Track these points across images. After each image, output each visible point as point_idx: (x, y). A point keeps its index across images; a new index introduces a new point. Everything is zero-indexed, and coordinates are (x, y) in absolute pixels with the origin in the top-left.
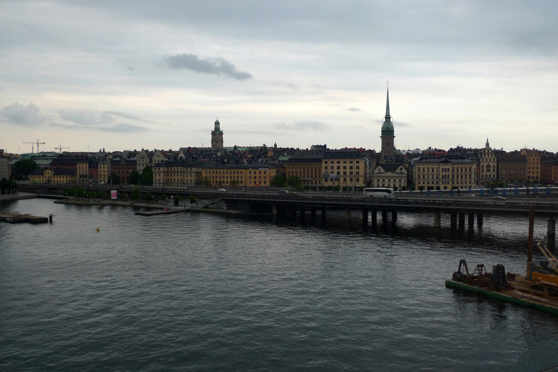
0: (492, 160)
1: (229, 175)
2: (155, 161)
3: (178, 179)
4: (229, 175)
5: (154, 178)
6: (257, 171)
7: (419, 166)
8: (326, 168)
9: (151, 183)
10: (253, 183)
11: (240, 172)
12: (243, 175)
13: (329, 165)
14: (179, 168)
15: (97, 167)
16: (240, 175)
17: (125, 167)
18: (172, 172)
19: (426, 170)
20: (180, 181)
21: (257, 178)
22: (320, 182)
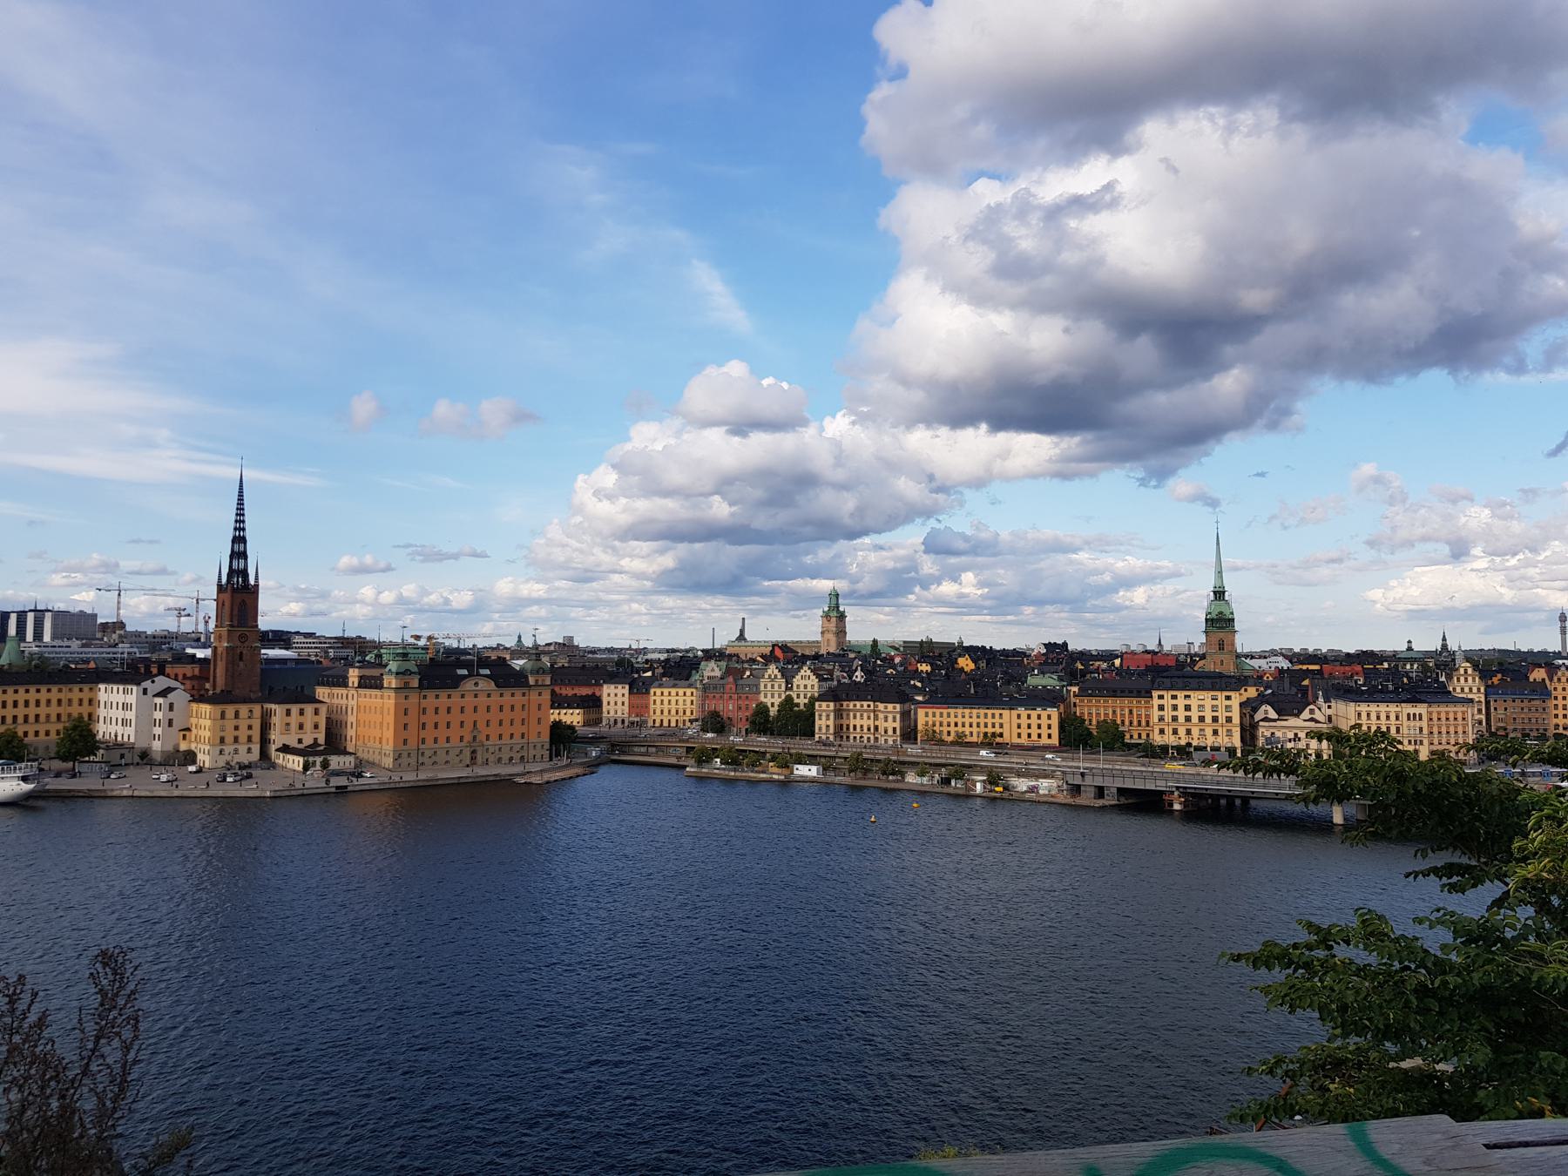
4: (975, 720)
5: (818, 723)
6: (1034, 714)
9: (810, 734)
10: (1024, 736)
13: (1168, 701)
19: (1373, 716)
21: (1034, 727)
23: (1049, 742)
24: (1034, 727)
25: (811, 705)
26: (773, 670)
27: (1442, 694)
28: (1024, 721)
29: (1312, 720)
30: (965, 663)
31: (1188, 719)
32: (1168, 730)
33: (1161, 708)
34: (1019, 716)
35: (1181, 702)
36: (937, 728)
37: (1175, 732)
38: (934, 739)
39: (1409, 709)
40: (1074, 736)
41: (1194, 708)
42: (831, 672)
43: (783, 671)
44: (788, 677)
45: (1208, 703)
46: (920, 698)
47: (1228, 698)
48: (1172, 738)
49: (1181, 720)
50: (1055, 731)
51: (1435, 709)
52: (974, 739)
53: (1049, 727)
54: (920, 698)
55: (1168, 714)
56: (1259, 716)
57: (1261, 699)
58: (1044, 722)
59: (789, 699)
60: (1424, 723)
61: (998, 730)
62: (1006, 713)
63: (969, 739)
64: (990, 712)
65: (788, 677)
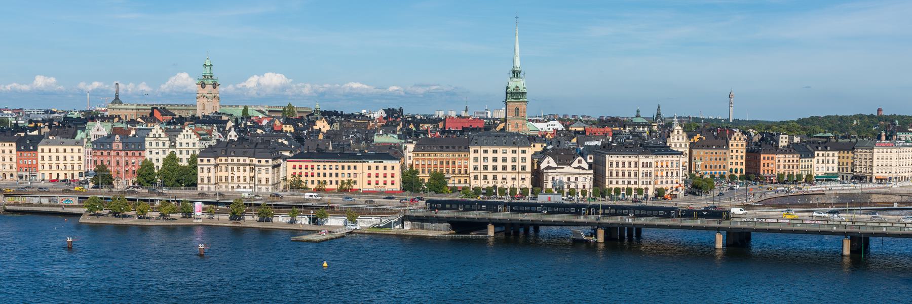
0: (683, 145)
1: (334, 172)
2: (181, 144)
3: (239, 177)
4: (334, 172)
5: (200, 175)
6: (381, 166)
10: (373, 183)
12: (358, 171)
13: (481, 155)
14: (242, 159)
15: (35, 150)
16: (352, 171)
17: (122, 154)
18: (228, 165)
20: (242, 181)
21: (381, 176)
24: (381, 176)
25: (193, 160)
26: (157, 129)
27: (665, 150)
28: (373, 172)
29: (579, 167)
30: (322, 125)
31: (495, 168)
32: (481, 176)
33: (476, 159)
34: (369, 168)
36: (303, 178)
37: (485, 178)
39: (643, 159)
42: (210, 133)
43: (167, 131)
45: (509, 156)
46: (287, 154)
47: (524, 152)
48: (483, 182)
49: (490, 168)
50: (397, 179)
51: (660, 158)
52: (334, 186)
54: (287, 154)
55: (481, 164)
56: (543, 165)
57: (544, 153)
58: (389, 172)
59: (172, 155)
60: (652, 169)
61: (352, 178)
62: (359, 165)
63: (328, 186)
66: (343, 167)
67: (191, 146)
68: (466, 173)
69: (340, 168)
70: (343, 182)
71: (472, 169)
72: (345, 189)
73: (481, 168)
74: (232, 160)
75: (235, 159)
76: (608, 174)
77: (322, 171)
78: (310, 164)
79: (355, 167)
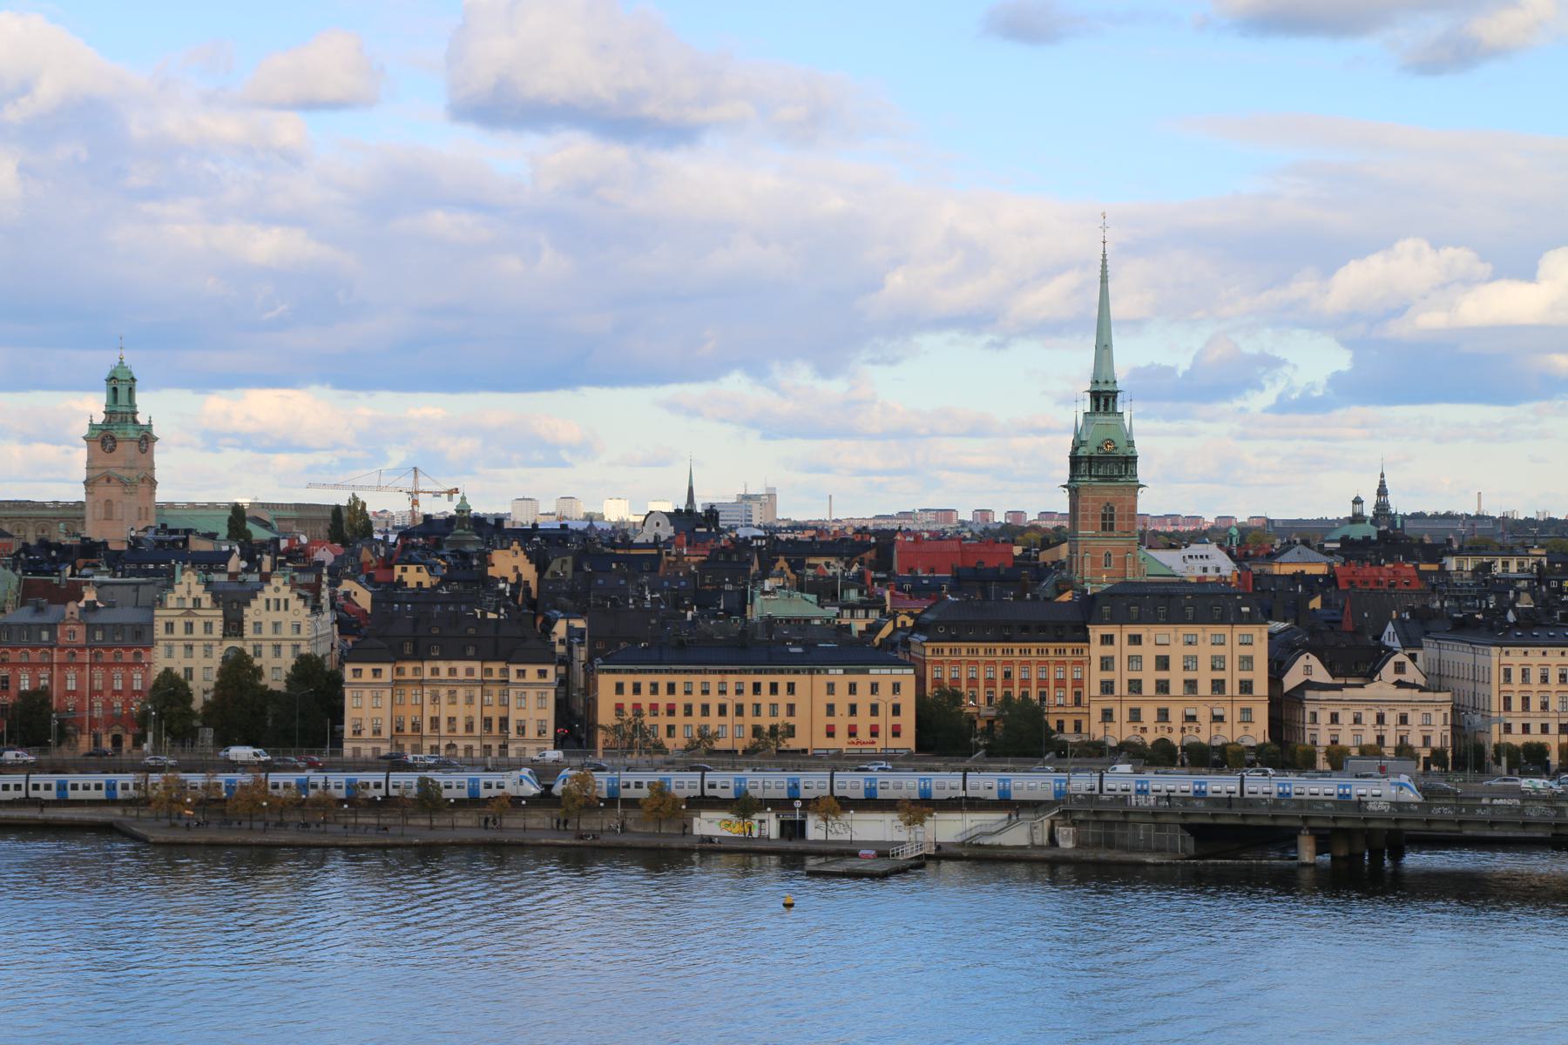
1: (731, 700)
2: (258, 626)
3: (451, 720)
6: (863, 682)
7: (1505, 660)
8: (1106, 663)
9: (338, 741)
11: (782, 688)
13: (1121, 649)
14: (461, 666)
16: (783, 698)
17: (86, 657)
18: (421, 683)
19: (1535, 676)
22: (1078, 727)
23: (895, 743)
24: (865, 710)
28: (842, 699)
29: (1400, 684)
31: (1163, 687)
32: (1121, 713)
34: (831, 688)
35: (1148, 652)
36: (648, 720)
37: (1135, 715)
38: (636, 739)
40: (942, 732)
41: (1176, 664)
44: (232, 605)
49: (1149, 688)
50: (908, 721)
53: (896, 710)
55: (1121, 676)
56: (1292, 680)
61: (782, 718)
64: (765, 680)
65: (232, 605)
66: (757, 688)
67: (287, 632)
68: (1078, 703)
69: (748, 689)
70: (757, 731)
71: (1096, 689)
72: (769, 746)
73: (1121, 688)
74: (435, 671)
75: (443, 666)
76: (1496, 705)
77: (697, 700)
78: (663, 680)
79: (791, 688)
